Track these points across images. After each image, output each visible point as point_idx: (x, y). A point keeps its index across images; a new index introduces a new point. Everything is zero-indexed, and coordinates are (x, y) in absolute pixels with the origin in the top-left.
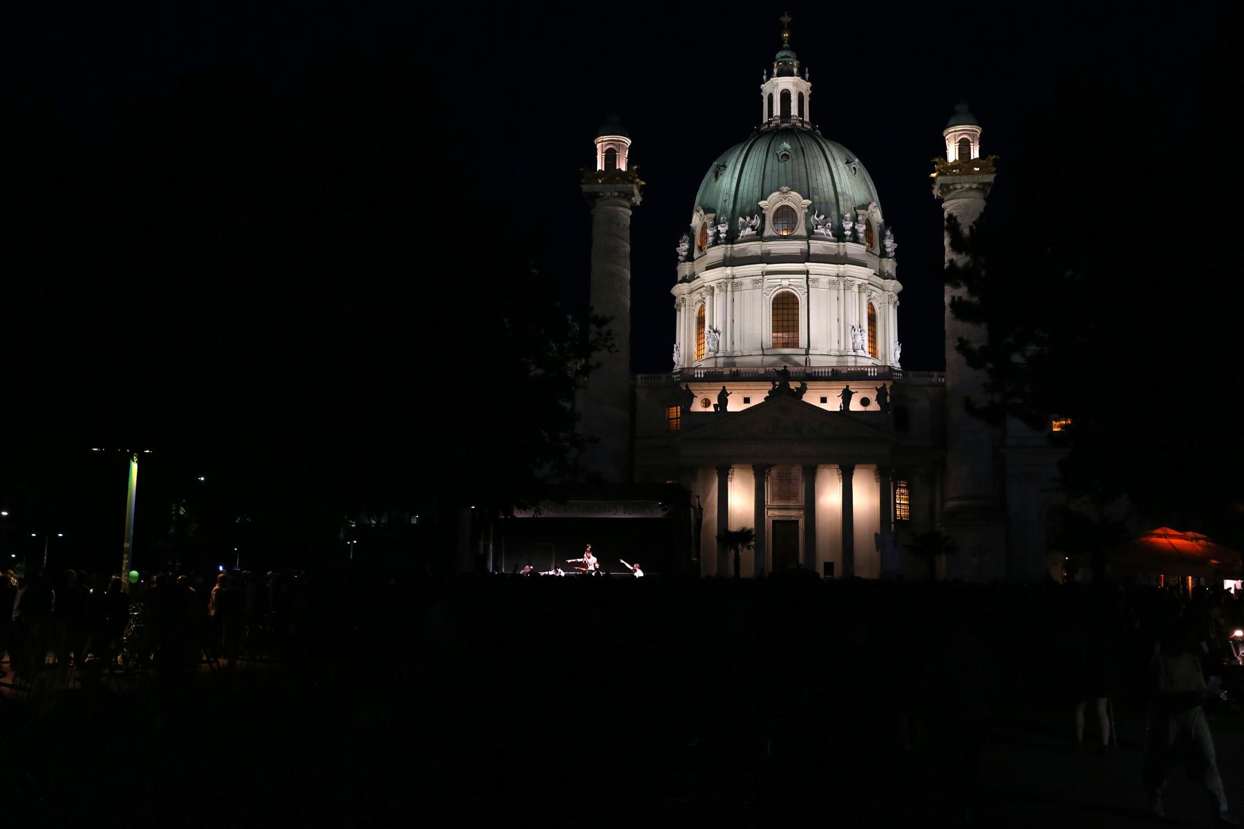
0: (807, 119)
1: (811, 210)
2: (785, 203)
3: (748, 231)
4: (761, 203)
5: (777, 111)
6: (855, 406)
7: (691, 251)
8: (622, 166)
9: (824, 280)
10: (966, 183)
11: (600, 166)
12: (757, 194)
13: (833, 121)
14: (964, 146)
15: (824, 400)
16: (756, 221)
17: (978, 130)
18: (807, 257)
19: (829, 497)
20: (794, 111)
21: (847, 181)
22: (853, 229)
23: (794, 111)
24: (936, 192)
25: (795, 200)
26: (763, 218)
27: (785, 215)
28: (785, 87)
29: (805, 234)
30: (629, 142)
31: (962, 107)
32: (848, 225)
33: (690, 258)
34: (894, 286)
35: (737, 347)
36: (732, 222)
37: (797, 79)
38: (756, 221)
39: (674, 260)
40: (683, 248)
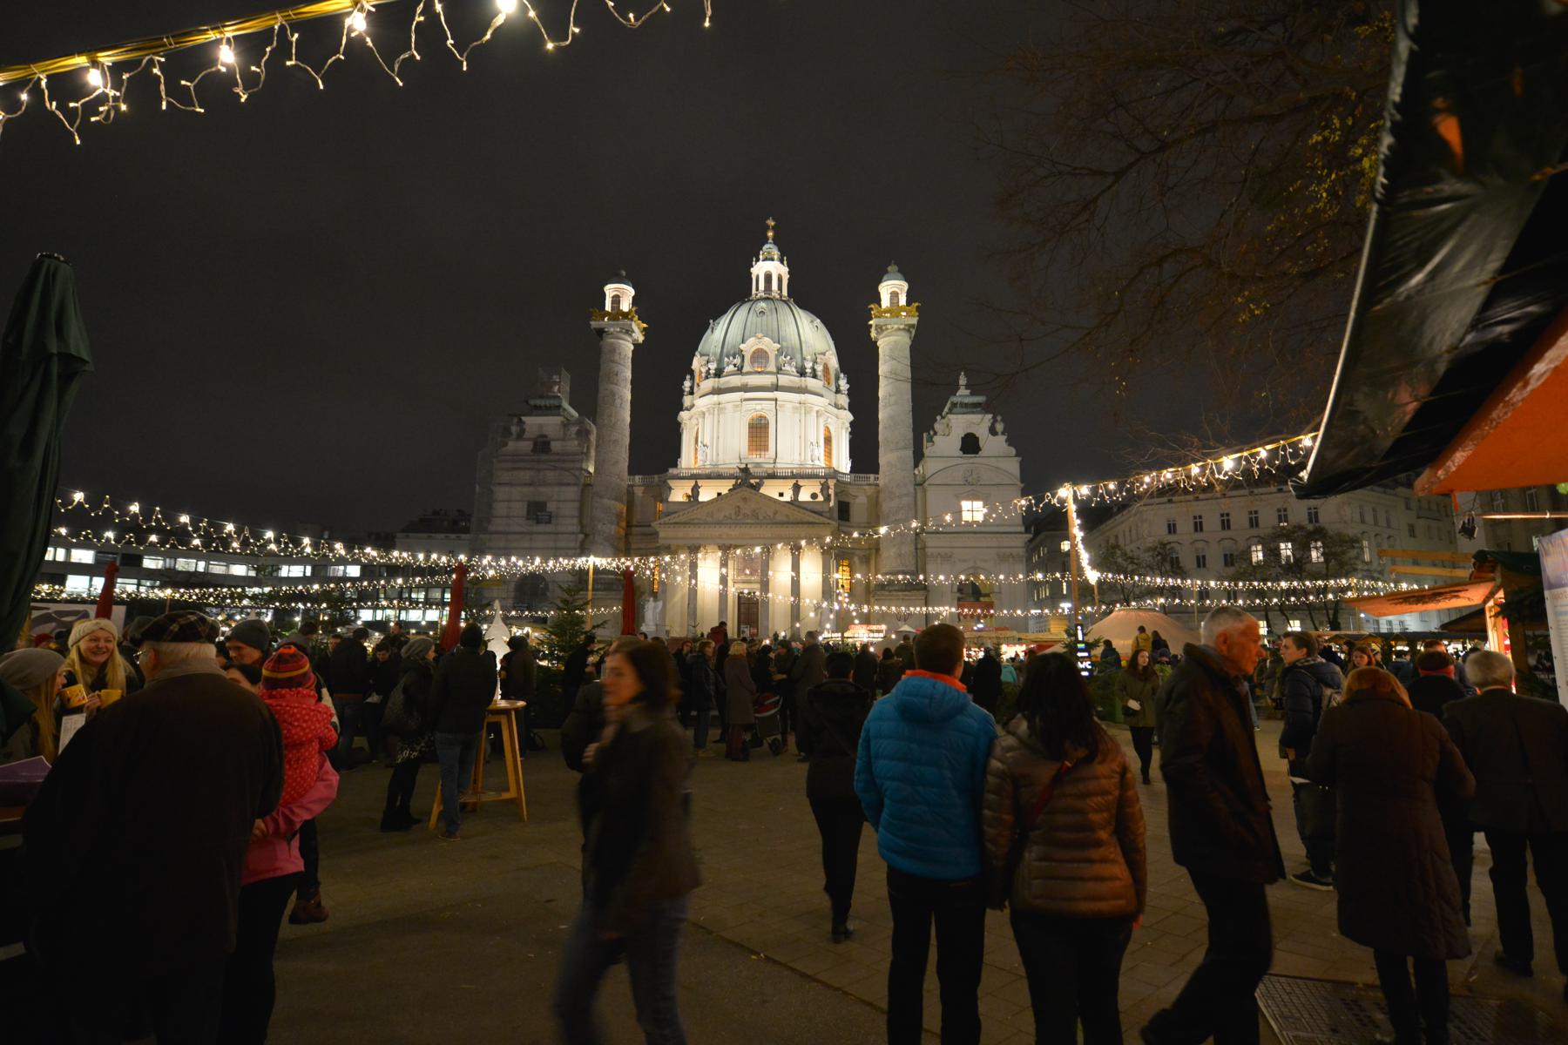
0: (785, 292)
1: (780, 352)
3: (731, 368)
5: (762, 286)
6: (804, 496)
8: (625, 306)
9: (789, 406)
10: (895, 324)
11: (608, 307)
13: (803, 294)
14: (894, 295)
15: (781, 495)
16: (738, 361)
17: (905, 286)
18: (776, 388)
19: (781, 573)
21: (811, 335)
22: (814, 370)
24: (873, 334)
26: (743, 358)
27: (760, 356)
28: (769, 268)
31: (892, 268)
32: (809, 365)
33: (692, 393)
36: (720, 361)
37: (777, 263)
39: (681, 393)
40: (687, 384)
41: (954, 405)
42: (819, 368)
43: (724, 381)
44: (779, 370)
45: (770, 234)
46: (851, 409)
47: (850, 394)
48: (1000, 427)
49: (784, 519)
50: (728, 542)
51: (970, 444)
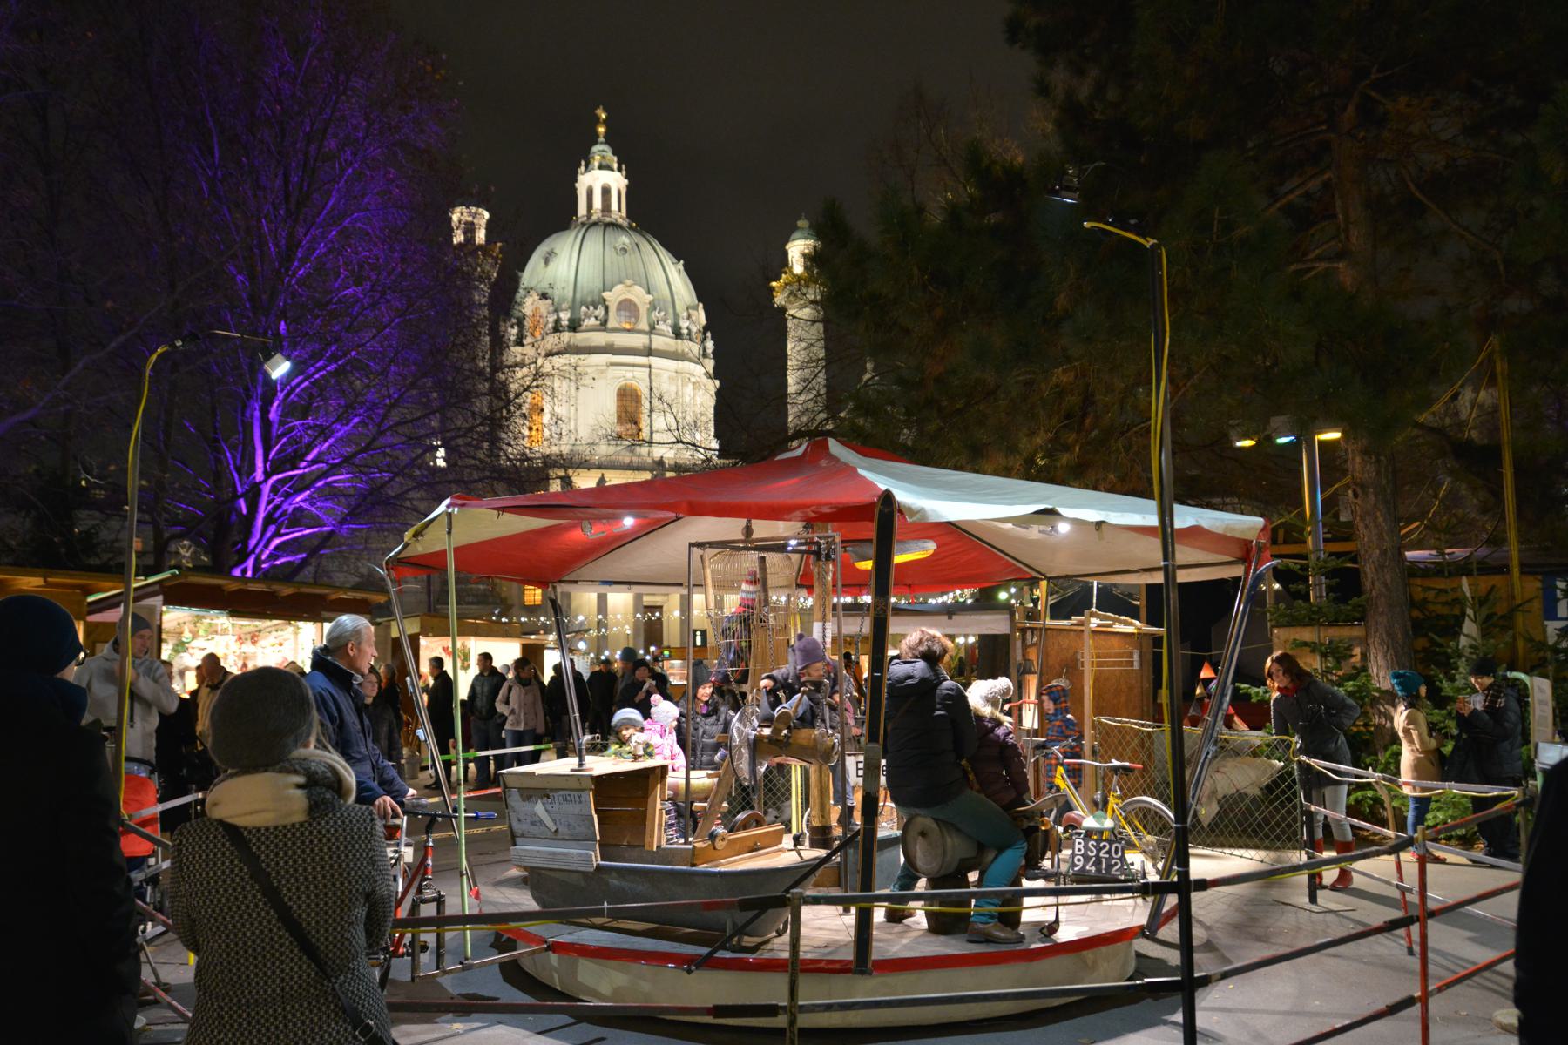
1: (653, 306)
3: (592, 321)
12: (599, 284)
16: (600, 311)
18: (649, 352)
20: (614, 206)
21: (670, 278)
25: (638, 295)
26: (607, 308)
29: (647, 328)
30: (487, 215)
33: (520, 343)
34: (713, 385)
36: (573, 307)
37: (617, 175)
38: (600, 311)
43: (580, 338)
45: (601, 130)
47: (716, 354)
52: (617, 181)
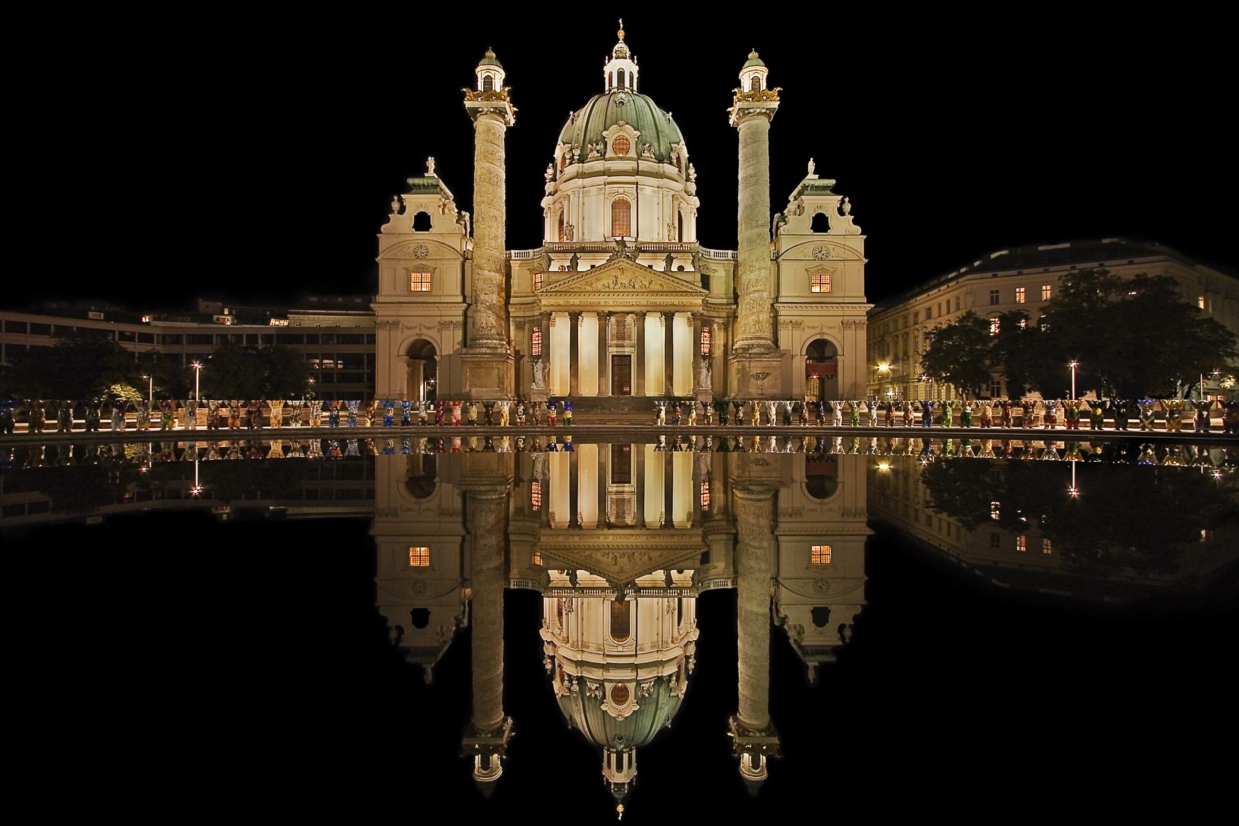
2: (621, 133)
4: (604, 134)
5: (615, 84)
7: (555, 175)
18: (637, 172)
20: (627, 84)
23: (627, 84)
26: (605, 144)
28: (621, 65)
33: (554, 179)
35: (586, 236)
39: (543, 182)
41: (805, 187)
42: (674, 156)
43: (588, 166)
44: (640, 157)
45: (621, 34)
46: (698, 194)
48: (847, 207)
49: (659, 288)
50: (606, 310)
51: (820, 224)
52: (631, 67)
